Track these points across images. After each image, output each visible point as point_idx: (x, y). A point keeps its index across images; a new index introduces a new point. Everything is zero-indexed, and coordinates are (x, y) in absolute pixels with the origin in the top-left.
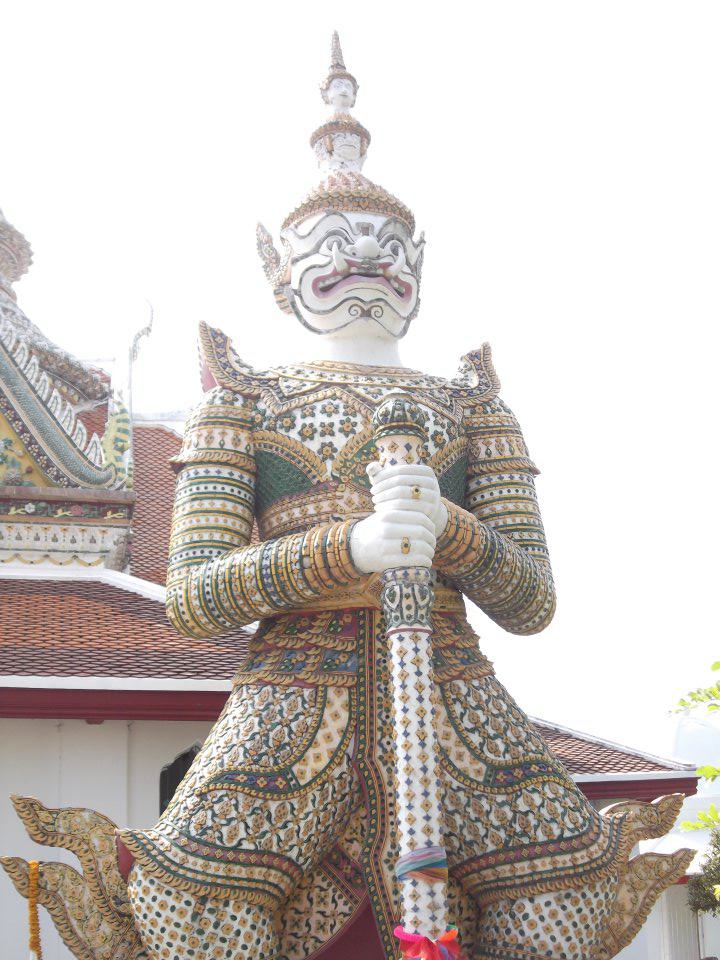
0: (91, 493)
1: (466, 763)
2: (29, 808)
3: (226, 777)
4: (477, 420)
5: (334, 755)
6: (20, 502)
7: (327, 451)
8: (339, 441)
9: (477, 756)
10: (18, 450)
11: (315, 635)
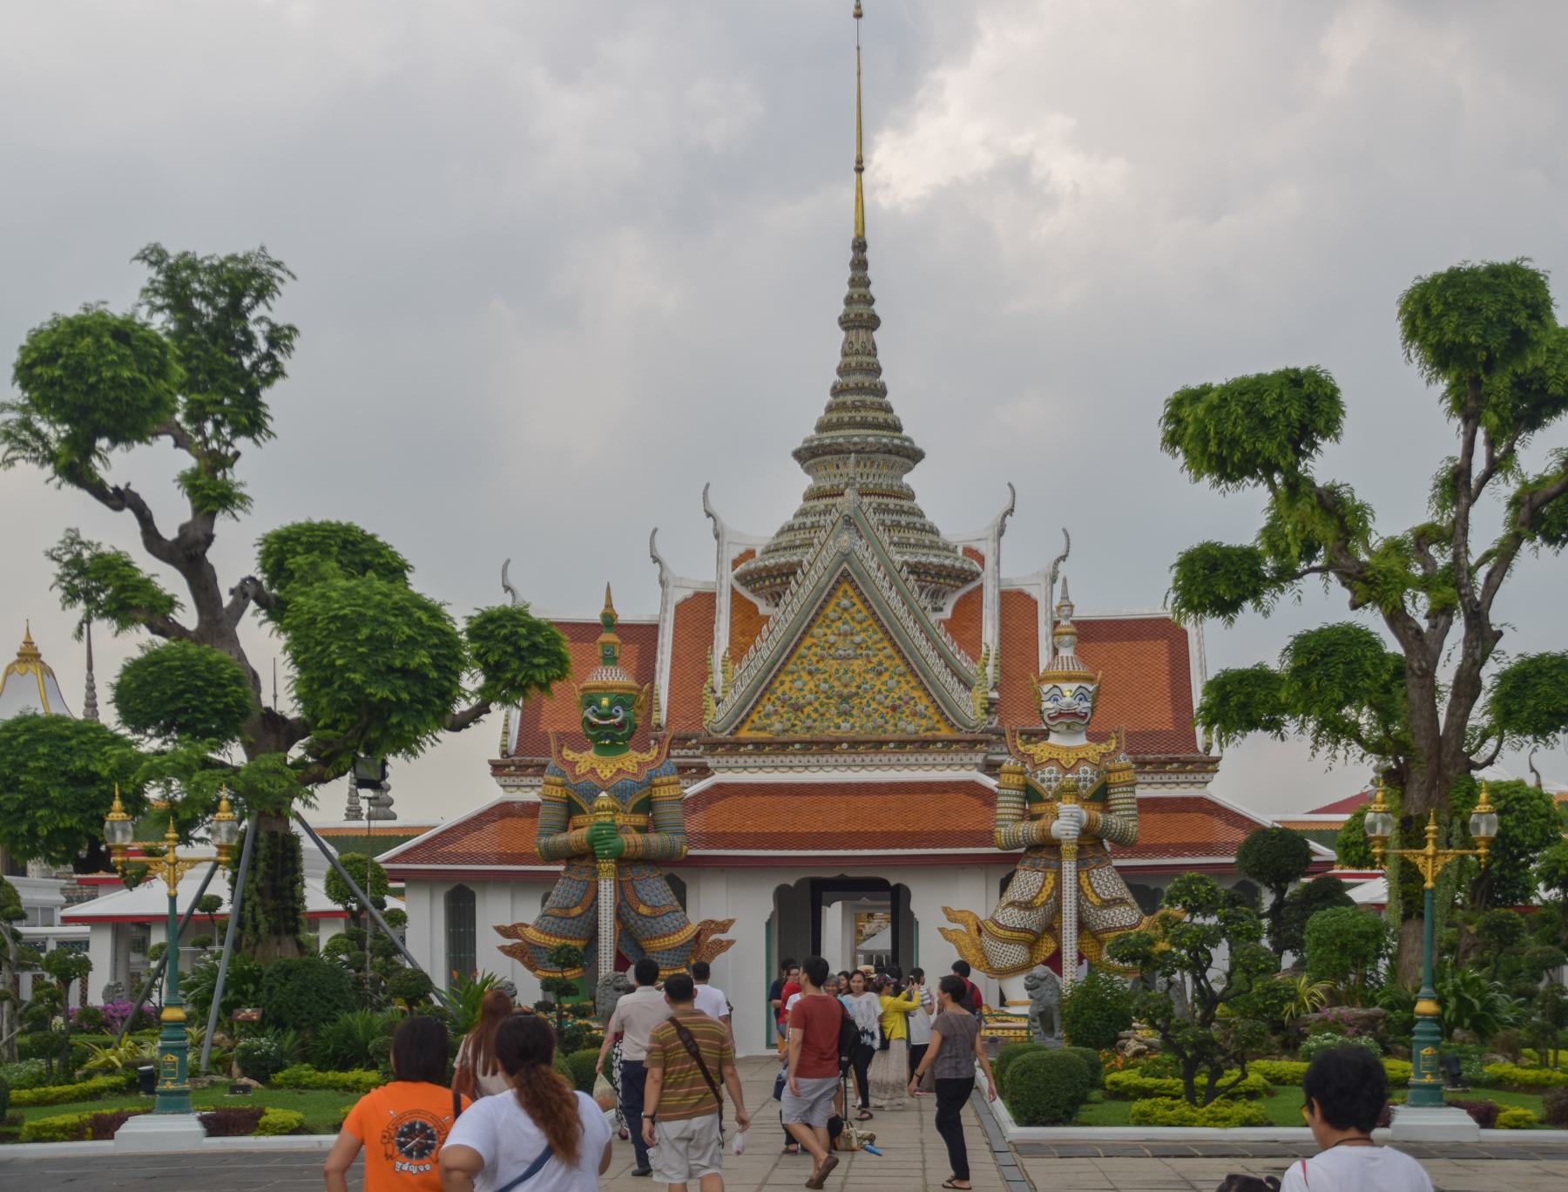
0: (969, 737)
1: (1094, 899)
2: (946, 910)
3: (1012, 904)
4: (1111, 766)
5: (1049, 897)
6: (935, 742)
7: (1050, 788)
8: (1054, 784)
9: (1098, 896)
10: (931, 710)
11: (1043, 853)
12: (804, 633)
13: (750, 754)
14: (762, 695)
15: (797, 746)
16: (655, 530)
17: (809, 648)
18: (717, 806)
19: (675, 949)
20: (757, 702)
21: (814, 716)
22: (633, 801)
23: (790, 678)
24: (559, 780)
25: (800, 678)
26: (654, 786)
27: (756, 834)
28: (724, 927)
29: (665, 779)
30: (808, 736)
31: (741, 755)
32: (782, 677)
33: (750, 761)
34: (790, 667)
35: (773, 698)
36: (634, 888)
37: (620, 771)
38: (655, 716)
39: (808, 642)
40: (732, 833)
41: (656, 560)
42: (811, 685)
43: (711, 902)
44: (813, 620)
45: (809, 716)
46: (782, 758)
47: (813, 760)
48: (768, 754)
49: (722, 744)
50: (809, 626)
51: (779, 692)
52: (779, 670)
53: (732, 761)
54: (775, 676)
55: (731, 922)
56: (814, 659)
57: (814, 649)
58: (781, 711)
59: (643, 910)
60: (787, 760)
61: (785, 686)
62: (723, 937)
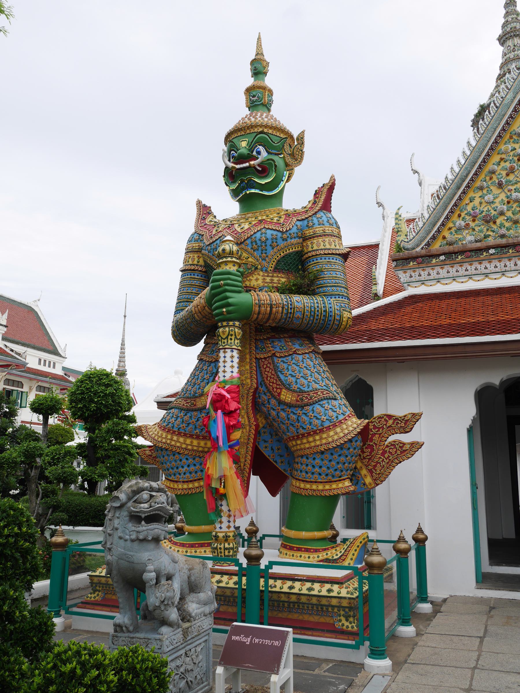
12: (492, 149)
13: (442, 265)
14: (452, 212)
15: (492, 251)
16: (379, 188)
17: (499, 164)
18: (409, 309)
19: (331, 451)
20: (447, 218)
21: (507, 224)
22: (274, 256)
23: (480, 193)
24: (196, 245)
25: (490, 192)
26: (305, 239)
27: (450, 325)
28: (407, 423)
29: (319, 230)
30: (504, 241)
31: (433, 267)
32: (471, 194)
33: (443, 273)
34: (478, 184)
35: (463, 215)
36: (276, 368)
37: (261, 221)
38: (374, 287)
39: (496, 158)
40: (422, 326)
41: (380, 204)
42: (503, 196)
43: (393, 399)
44: (499, 136)
45: (502, 226)
46: (476, 265)
47: (510, 264)
48: (461, 264)
49: (414, 258)
50: (496, 142)
51: (469, 208)
52: (468, 186)
53: (424, 275)
54: (464, 192)
55: (416, 417)
56: (504, 173)
57: (502, 164)
58: (472, 224)
59: (287, 396)
60: (481, 268)
61: (475, 202)
62: (406, 438)
